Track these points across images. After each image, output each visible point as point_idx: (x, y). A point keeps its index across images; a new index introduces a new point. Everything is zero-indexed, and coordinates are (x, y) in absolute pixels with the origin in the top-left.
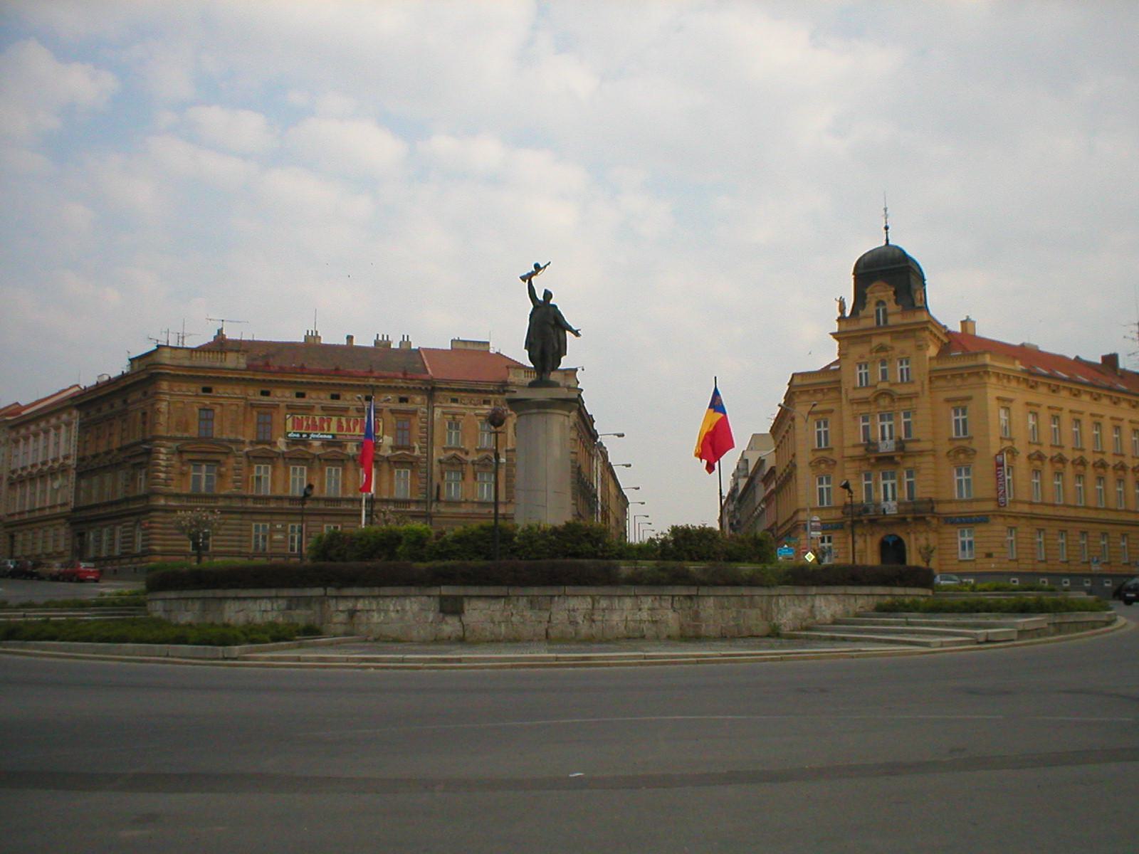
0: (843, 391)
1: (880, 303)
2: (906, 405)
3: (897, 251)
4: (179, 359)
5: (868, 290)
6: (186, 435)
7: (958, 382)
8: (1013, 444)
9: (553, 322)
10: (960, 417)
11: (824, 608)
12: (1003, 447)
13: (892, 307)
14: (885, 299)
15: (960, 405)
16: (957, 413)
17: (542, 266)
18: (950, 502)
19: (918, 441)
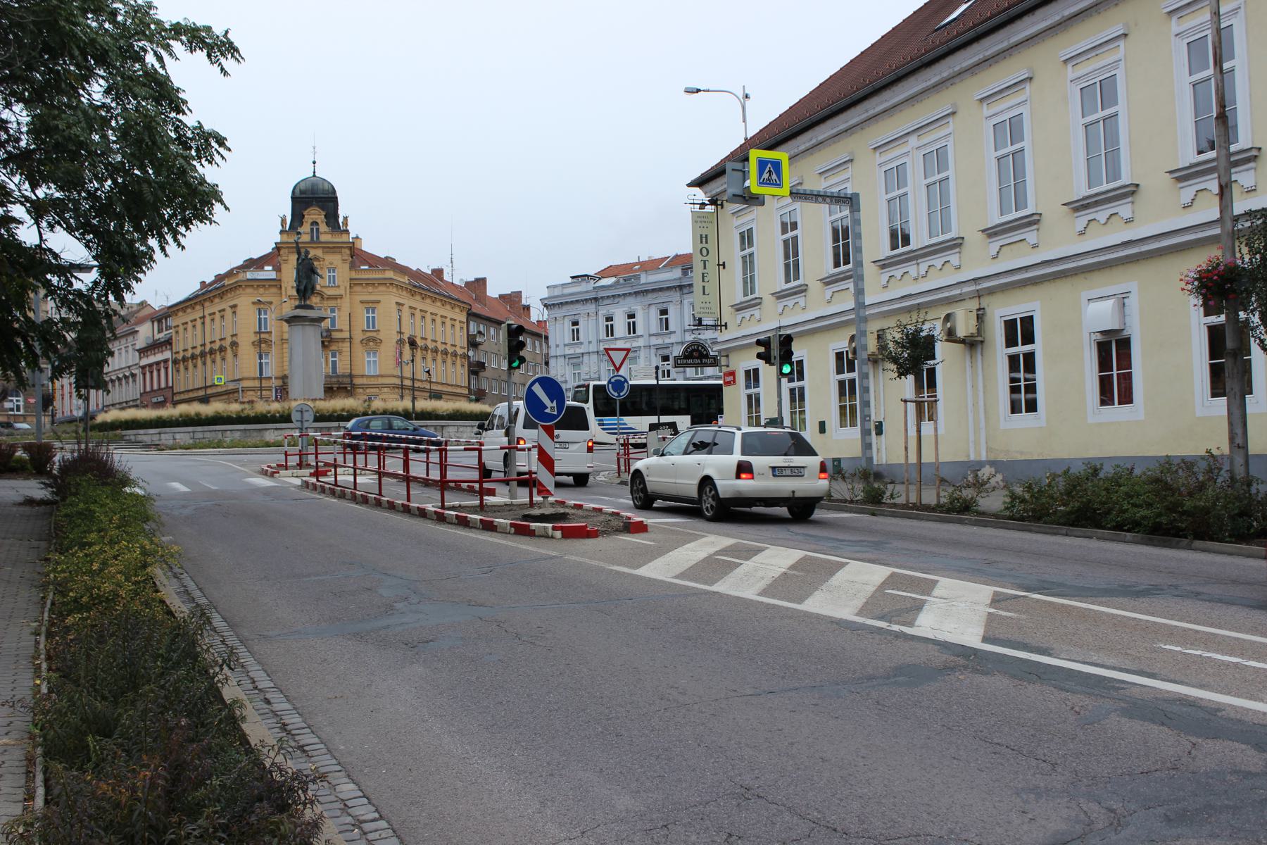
0: (283, 289)
1: (315, 223)
2: (332, 303)
5: (305, 213)
7: (370, 289)
10: (371, 315)
13: (323, 227)
14: (319, 221)
15: (371, 306)
18: (363, 376)
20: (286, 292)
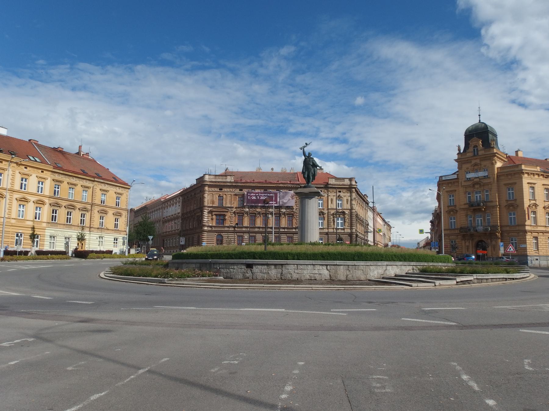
0: (460, 183)
3: (483, 125)
4: (211, 179)
5: (470, 142)
6: (214, 205)
7: (510, 177)
8: (536, 202)
9: (312, 164)
10: (511, 192)
11: (390, 270)
12: (530, 204)
16: (509, 190)
17: (308, 143)
18: (507, 226)
19: (492, 202)
20: (461, 184)
